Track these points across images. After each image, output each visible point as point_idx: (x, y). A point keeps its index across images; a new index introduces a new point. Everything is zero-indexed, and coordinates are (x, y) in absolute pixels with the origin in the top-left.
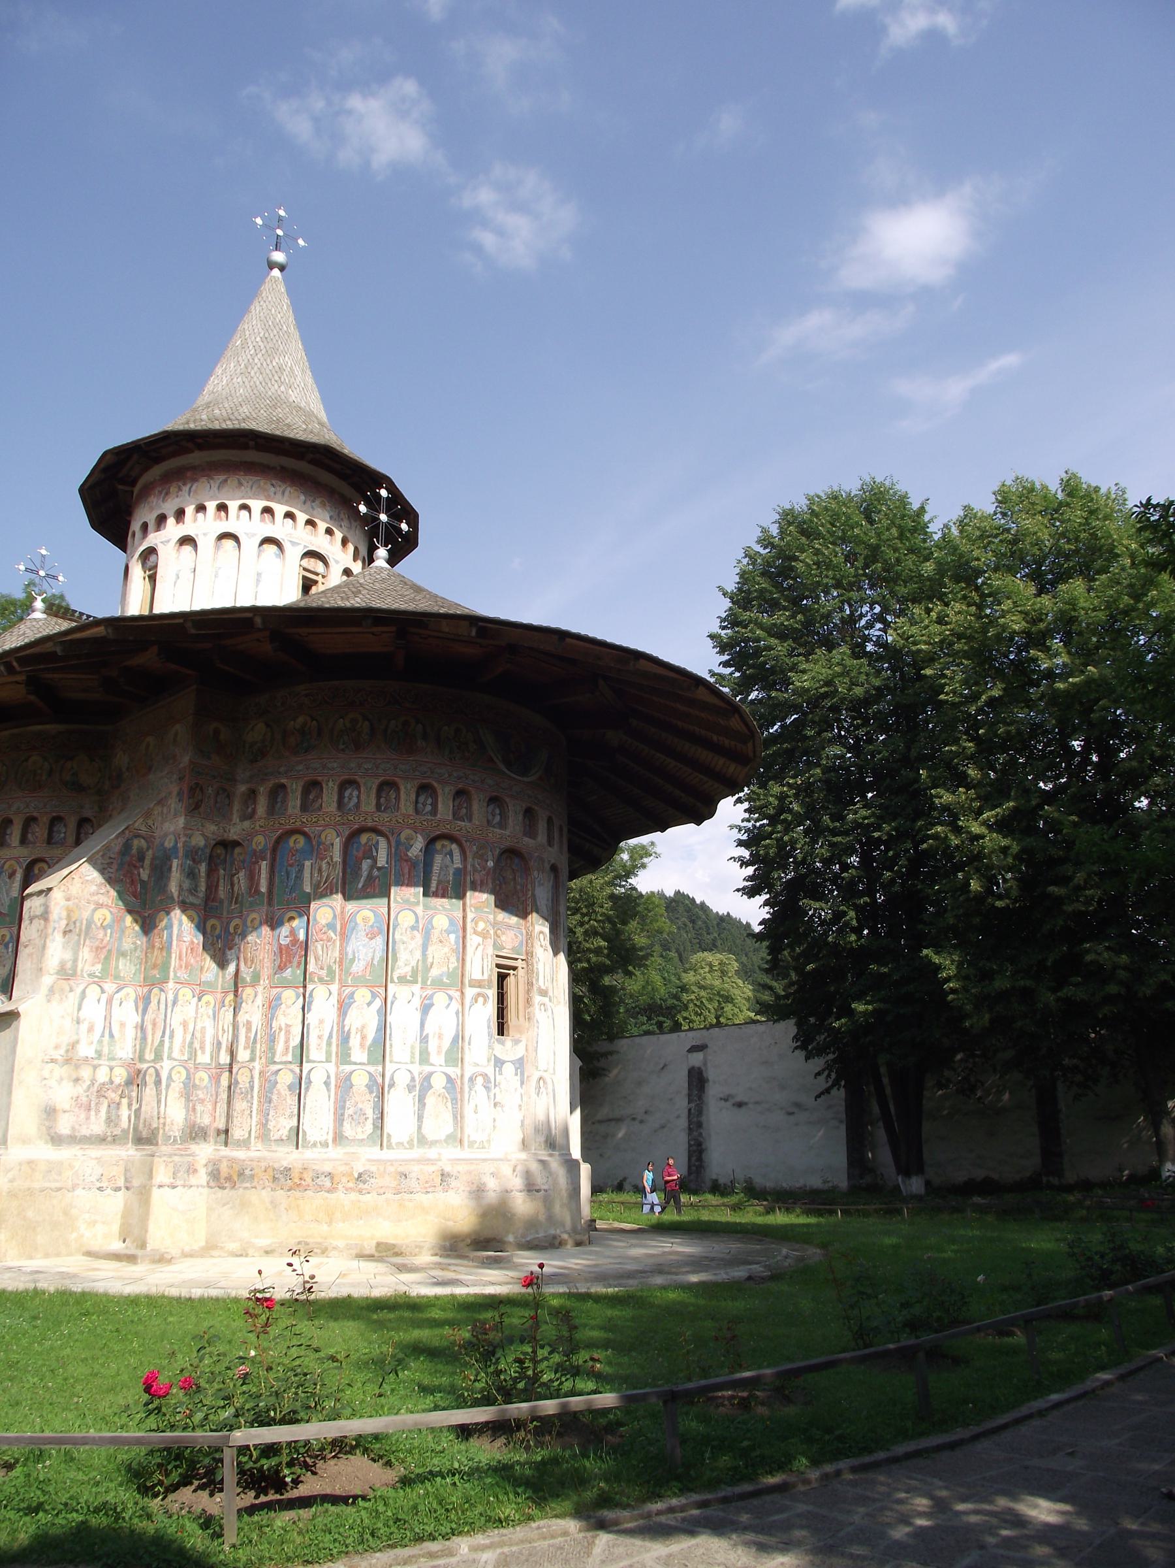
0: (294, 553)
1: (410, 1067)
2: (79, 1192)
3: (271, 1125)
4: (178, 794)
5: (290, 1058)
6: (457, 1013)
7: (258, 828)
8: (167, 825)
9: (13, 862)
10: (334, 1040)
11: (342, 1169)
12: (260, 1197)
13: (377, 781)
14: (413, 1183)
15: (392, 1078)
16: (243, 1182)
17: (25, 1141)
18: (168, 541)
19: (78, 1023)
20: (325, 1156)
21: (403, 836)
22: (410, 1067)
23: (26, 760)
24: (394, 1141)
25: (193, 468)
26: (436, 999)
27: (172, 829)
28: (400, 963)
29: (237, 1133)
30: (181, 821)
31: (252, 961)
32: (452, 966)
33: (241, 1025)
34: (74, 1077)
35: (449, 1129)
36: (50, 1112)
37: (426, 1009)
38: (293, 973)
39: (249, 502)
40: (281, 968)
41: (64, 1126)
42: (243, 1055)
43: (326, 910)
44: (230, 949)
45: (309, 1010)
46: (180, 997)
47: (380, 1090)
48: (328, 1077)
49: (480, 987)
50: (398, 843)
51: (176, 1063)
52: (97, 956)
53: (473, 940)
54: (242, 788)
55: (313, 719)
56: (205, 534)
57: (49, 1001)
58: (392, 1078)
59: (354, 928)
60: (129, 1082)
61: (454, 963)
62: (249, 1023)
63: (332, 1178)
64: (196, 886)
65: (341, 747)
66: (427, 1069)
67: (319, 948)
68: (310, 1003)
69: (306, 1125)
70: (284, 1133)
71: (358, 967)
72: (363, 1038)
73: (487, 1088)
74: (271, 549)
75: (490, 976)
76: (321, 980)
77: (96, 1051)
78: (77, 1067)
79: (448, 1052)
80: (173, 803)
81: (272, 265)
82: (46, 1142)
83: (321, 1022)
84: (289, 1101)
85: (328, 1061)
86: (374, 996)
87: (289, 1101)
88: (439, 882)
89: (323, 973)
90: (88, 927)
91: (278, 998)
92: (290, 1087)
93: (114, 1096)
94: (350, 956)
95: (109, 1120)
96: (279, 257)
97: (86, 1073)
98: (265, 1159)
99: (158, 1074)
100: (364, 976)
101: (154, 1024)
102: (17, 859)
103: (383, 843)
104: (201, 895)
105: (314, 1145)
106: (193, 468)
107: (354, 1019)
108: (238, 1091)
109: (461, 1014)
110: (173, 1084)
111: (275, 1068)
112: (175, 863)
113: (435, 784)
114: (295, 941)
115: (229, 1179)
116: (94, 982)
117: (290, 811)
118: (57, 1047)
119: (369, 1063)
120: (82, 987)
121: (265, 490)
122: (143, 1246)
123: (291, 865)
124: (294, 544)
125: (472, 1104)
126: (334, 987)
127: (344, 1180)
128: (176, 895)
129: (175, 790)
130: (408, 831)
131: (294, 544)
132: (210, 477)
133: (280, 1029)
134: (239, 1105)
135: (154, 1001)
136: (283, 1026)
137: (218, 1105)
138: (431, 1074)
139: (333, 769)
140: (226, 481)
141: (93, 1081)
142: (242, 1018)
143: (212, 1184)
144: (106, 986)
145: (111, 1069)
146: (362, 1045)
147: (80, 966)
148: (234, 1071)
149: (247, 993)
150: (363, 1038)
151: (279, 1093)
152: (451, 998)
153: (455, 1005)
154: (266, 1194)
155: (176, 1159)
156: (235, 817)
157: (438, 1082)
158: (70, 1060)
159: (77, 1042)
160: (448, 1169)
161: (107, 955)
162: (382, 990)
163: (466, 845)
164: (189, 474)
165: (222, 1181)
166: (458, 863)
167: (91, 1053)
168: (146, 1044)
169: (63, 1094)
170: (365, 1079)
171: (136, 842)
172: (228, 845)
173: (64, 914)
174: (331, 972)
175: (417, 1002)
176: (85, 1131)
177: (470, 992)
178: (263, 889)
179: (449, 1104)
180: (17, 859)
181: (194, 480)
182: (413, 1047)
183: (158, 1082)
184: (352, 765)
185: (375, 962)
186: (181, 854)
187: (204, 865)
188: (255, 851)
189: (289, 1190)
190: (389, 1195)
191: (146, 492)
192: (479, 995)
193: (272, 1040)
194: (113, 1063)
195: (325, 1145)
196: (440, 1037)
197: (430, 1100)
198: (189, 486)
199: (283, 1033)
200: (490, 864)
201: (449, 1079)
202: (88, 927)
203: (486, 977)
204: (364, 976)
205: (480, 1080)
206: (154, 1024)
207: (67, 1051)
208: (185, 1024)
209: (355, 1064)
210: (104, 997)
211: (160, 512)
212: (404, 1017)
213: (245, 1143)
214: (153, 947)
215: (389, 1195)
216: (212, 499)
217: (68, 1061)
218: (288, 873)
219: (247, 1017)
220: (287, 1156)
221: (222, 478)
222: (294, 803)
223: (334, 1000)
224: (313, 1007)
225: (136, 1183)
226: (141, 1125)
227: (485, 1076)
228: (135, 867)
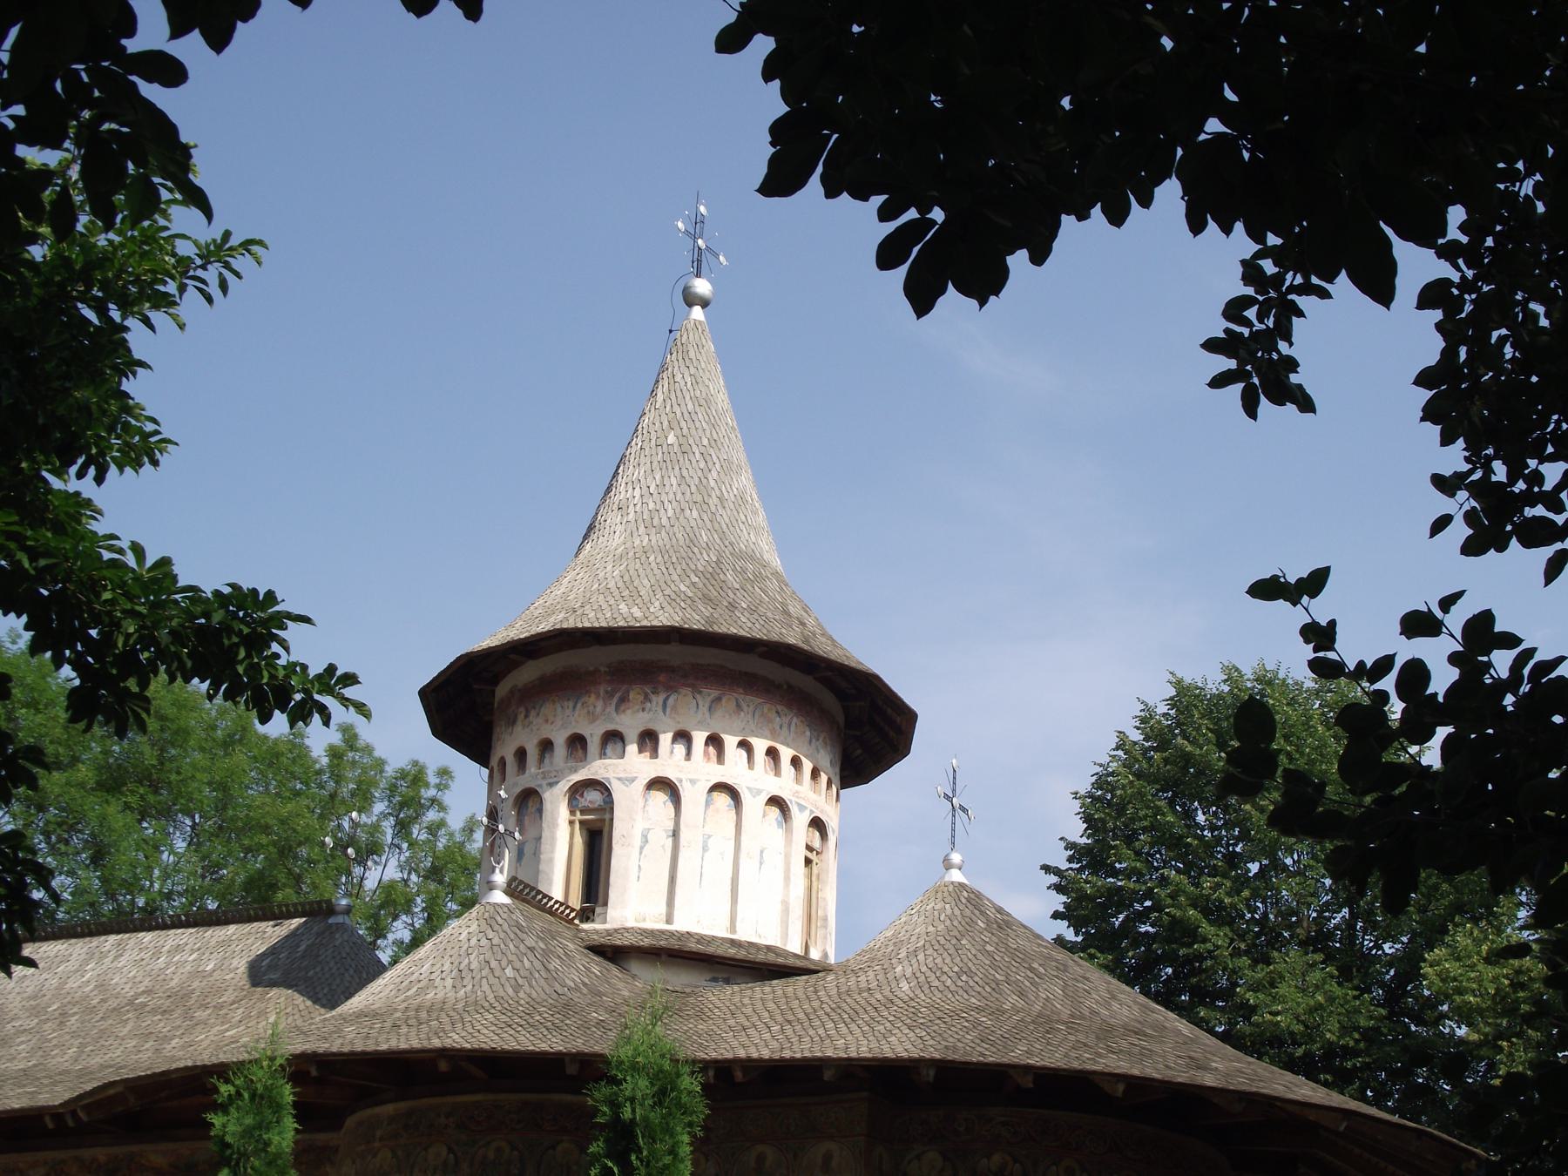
0: (801, 820)
18: (633, 780)
23: (553, 1147)
25: (670, 670)
39: (754, 741)
56: (693, 782)
74: (775, 812)
81: (690, 299)
96: (702, 287)
106: (670, 670)
121: (770, 721)
124: (802, 808)
131: (802, 808)
132: (696, 690)
140: (719, 699)
164: (662, 678)
181: (671, 688)
191: (568, 685)
211: (611, 727)
216: (701, 725)
221: (715, 693)
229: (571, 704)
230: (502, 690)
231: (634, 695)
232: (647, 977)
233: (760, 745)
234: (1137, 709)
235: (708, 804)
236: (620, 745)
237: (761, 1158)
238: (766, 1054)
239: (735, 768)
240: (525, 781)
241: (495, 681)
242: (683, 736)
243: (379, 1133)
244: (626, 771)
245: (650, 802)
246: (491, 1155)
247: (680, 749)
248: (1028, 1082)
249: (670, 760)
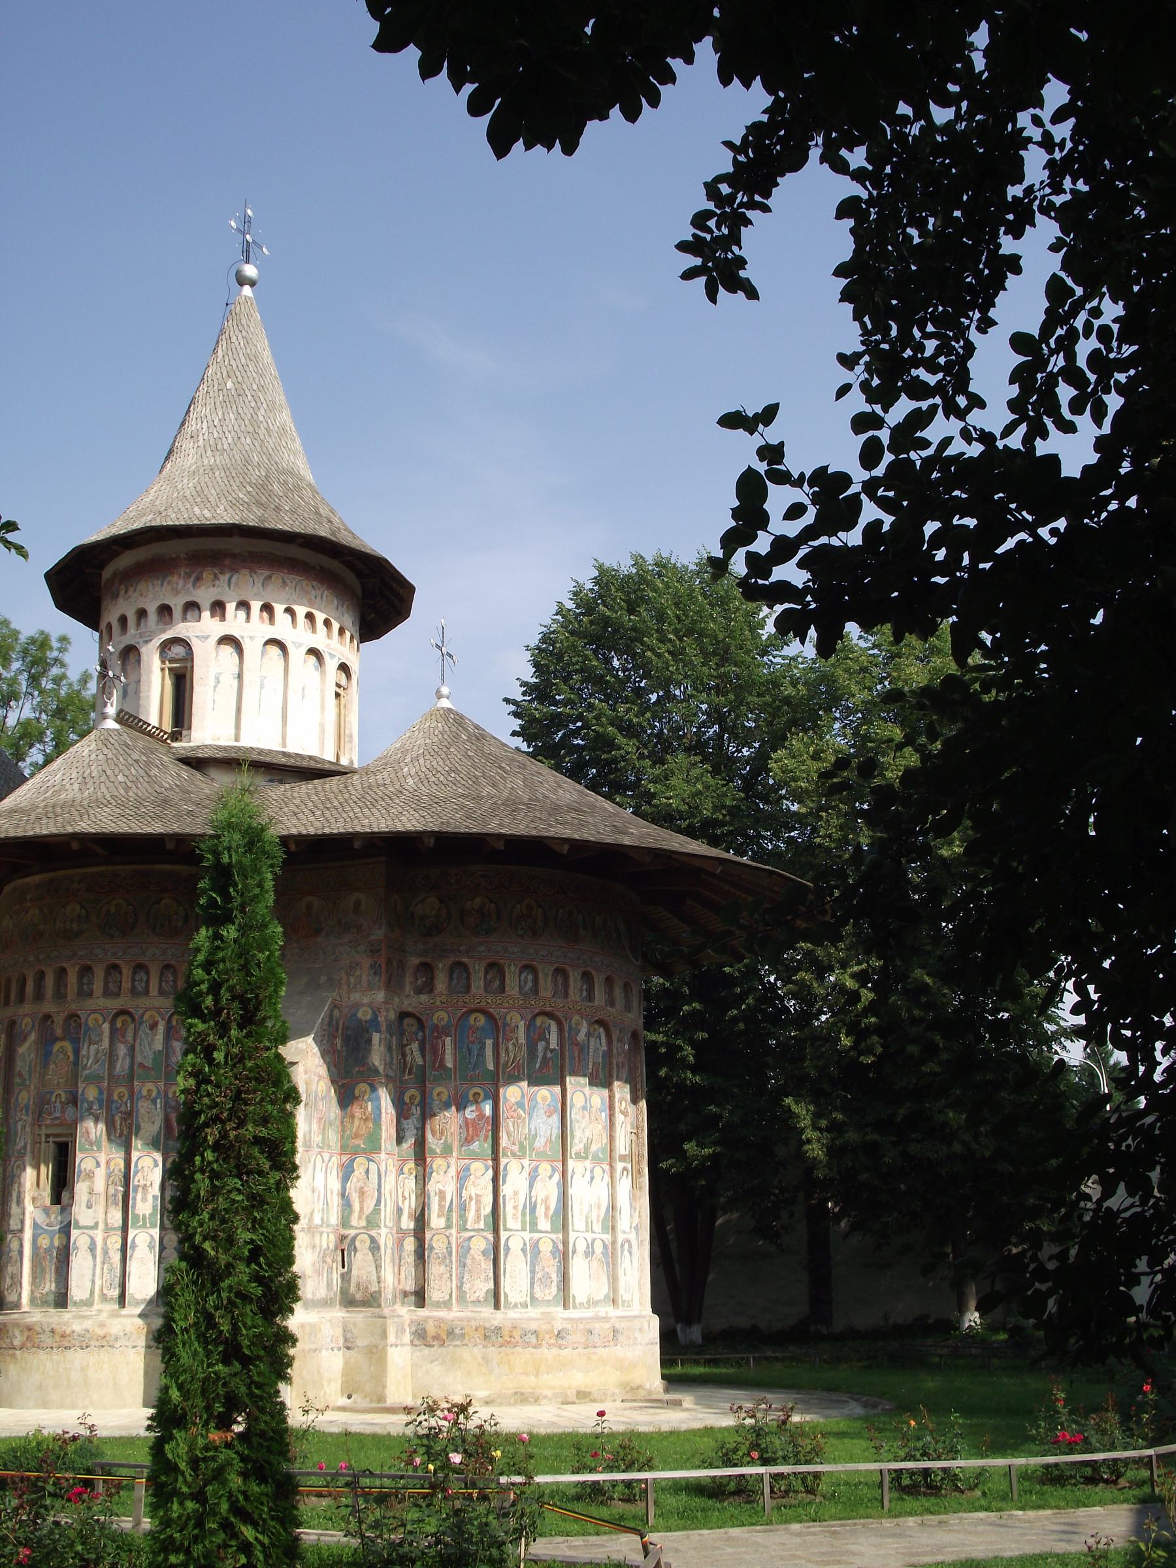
0: (331, 665)
2: (324, 1352)
3: (466, 1287)
4: (372, 967)
5: (482, 1225)
7: (438, 1003)
8: (355, 997)
9: (153, 1012)
11: (545, 1327)
12: (471, 1354)
13: (552, 968)
14: (596, 1339)
16: (453, 1340)
18: (207, 637)
20: (526, 1316)
21: (573, 1021)
23: (158, 902)
24: (577, 1301)
25: (234, 556)
27: (366, 1000)
28: (576, 1141)
29: (435, 1293)
30: (380, 996)
31: (442, 1134)
33: (432, 1194)
35: (605, 1290)
38: (481, 1146)
39: (296, 608)
40: (468, 1141)
42: (436, 1221)
43: (512, 1093)
44: (406, 1118)
45: (504, 1182)
47: (564, 1257)
48: (525, 1244)
50: (570, 1028)
53: (619, 1118)
54: (416, 961)
55: (491, 902)
56: (252, 638)
61: (605, 1140)
62: (442, 1195)
63: (537, 1336)
65: (520, 932)
66: (594, 1236)
67: (511, 1124)
68: (505, 1176)
69: (506, 1285)
70: (481, 1294)
71: (540, 1143)
72: (547, 1208)
76: (514, 1155)
80: (365, 975)
81: (242, 280)
83: (516, 1193)
84: (484, 1266)
85: (523, 1229)
86: (554, 1170)
87: (484, 1266)
88: (594, 1063)
89: (516, 1148)
91: (467, 1169)
92: (484, 1253)
93: (329, 1260)
96: (250, 271)
98: (475, 1320)
99: (373, 1240)
101: (362, 1193)
102: (157, 1009)
103: (554, 1028)
105: (516, 1306)
106: (234, 556)
108: (433, 1255)
109: (613, 1185)
111: (467, 1234)
112: (376, 1037)
113: (593, 972)
114: (481, 1116)
115: (437, 1337)
117: (474, 990)
119: (553, 1231)
121: (307, 593)
122: (381, 1398)
123: (473, 1042)
124: (332, 656)
126: (526, 1162)
127: (547, 1337)
128: (381, 1069)
129: (366, 962)
130: (576, 1018)
131: (332, 656)
132: (252, 571)
133: (471, 1198)
134: (435, 1269)
135: (359, 1172)
136: (473, 1196)
137: (403, 1269)
138: (594, 1241)
139: (514, 953)
140: (269, 577)
142: (432, 1187)
143: (416, 1342)
146: (546, 1215)
148: (428, 1236)
149: (437, 1164)
150: (547, 1208)
151: (473, 1258)
153: (607, 1178)
154: (477, 1351)
156: (408, 989)
160: (617, 1326)
162: (559, 1165)
163: (612, 1029)
164: (227, 562)
165: (429, 1339)
166: (605, 1048)
167: (319, 1223)
168: (351, 1212)
170: (550, 1248)
172: (403, 1015)
174: (522, 1147)
175: (588, 1175)
176: (318, 1296)
177: (619, 1166)
178: (450, 1065)
180: (157, 1009)
181: (234, 570)
183: (375, 1246)
184: (531, 951)
186: (384, 1028)
188: (436, 1026)
190: (580, 1350)
191: (157, 568)
193: (463, 1208)
195: (525, 1305)
196: (599, 1208)
198: (227, 576)
199: (473, 1203)
200: (626, 1047)
204: (545, 1151)
206: (362, 1193)
211: (190, 599)
212: (578, 1189)
213: (447, 1305)
214: (352, 1116)
215: (580, 1350)
216: (257, 597)
218: (469, 1050)
219: (440, 1186)
220: (497, 1318)
221: (266, 573)
222: (478, 984)
223: (525, 1174)
224: (508, 1179)
225: (360, 1343)
226: (352, 1289)
229: (159, 582)
230: (107, 574)
231: (207, 575)
232: (222, 780)
233: (301, 611)
234: (571, 586)
235: (263, 653)
236: (197, 612)
237: (309, 906)
238: (312, 831)
239: (282, 627)
240: (127, 640)
241: (102, 566)
242: (244, 605)
243: (29, 897)
244: (202, 631)
245: (220, 653)
246: (113, 910)
247: (242, 614)
248: (501, 846)
249: (234, 622)
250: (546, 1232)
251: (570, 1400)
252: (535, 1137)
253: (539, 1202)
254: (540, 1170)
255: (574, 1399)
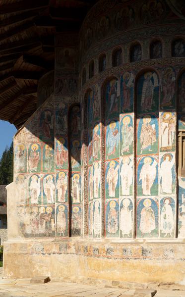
1: (130, 197)
2: (34, 255)
6: (157, 167)
10: (101, 187)
14: (129, 254)
15: (122, 203)
17: (14, 236)
19: (29, 191)
22: (130, 197)
24: (123, 234)
26: (145, 161)
28: (124, 145)
32: (153, 142)
34: (30, 212)
36: (22, 225)
37: (137, 167)
41: (28, 230)
46: (60, 176)
49: (167, 151)
51: (59, 204)
52: (34, 164)
57: (17, 183)
58: (122, 203)
59: (108, 131)
60: (53, 213)
61: (154, 140)
64: (63, 127)
71: (110, 151)
72: (113, 185)
73: (172, 206)
75: (173, 144)
77: (38, 201)
78: (31, 208)
79: (153, 187)
82: (22, 237)
83: (97, 179)
86: (117, 163)
90: (29, 152)
94: (108, 146)
95: (47, 228)
97: (35, 210)
100: (113, 154)
104: (66, 130)
107: (109, 177)
110: (59, 212)
116: (34, 174)
118: (22, 201)
120: (30, 176)
125: (163, 214)
138: (143, 200)
141: (38, 213)
144: (40, 176)
145: (46, 208)
146: (113, 189)
147: (28, 168)
150: (113, 185)
152: (153, 159)
155: (61, 243)
157: (147, 204)
158: (28, 205)
159: (30, 198)
160: (145, 247)
161: (39, 162)
167: (36, 202)
169: (27, 219)
171: (46, 113)
173: (19, 148)
175: (132, 163)
176: (37, 232)
179: (153, 215)
182: (130, 187)
185: (117, 147)
187: (66, 116)
189: (87, 256)
192: (166, 155)
194: (46, 206)
196: (147, 181)
197: (143, 213)
201: (152, 200)
202: (29, 152)
203: (171, 145)
204: (113, 154)
205: (167, 202)
207: (26, 202)
208: (63, 187)
209: (111, 198)
210: (39, 180)
215: (118, 260)
217: (27, 206)
227: (171, 199)
228: (47, 124)
250: (113, 198)
251: (109, 285)
252: (108, 148)
253: (109, 182)
254: (110, 165)
255: (111, 285)
